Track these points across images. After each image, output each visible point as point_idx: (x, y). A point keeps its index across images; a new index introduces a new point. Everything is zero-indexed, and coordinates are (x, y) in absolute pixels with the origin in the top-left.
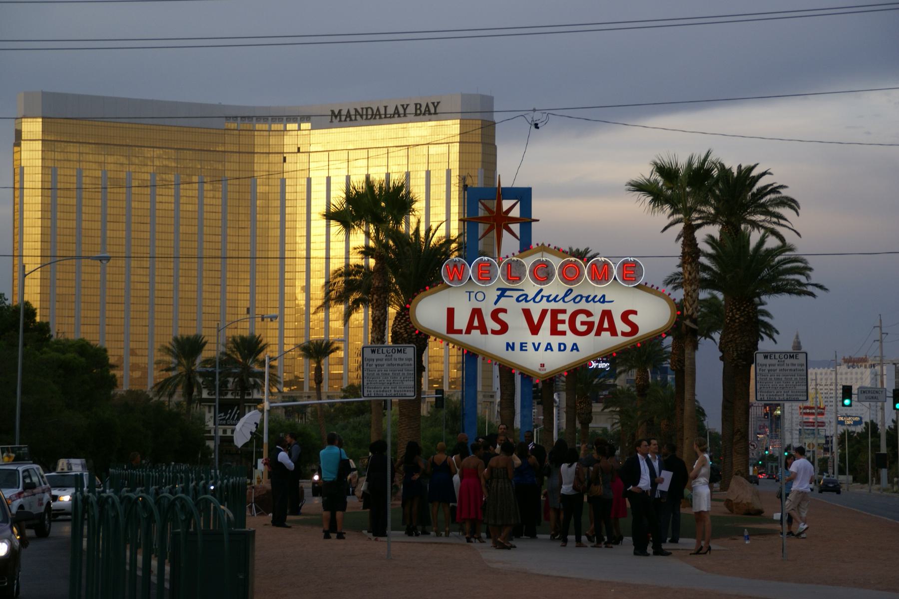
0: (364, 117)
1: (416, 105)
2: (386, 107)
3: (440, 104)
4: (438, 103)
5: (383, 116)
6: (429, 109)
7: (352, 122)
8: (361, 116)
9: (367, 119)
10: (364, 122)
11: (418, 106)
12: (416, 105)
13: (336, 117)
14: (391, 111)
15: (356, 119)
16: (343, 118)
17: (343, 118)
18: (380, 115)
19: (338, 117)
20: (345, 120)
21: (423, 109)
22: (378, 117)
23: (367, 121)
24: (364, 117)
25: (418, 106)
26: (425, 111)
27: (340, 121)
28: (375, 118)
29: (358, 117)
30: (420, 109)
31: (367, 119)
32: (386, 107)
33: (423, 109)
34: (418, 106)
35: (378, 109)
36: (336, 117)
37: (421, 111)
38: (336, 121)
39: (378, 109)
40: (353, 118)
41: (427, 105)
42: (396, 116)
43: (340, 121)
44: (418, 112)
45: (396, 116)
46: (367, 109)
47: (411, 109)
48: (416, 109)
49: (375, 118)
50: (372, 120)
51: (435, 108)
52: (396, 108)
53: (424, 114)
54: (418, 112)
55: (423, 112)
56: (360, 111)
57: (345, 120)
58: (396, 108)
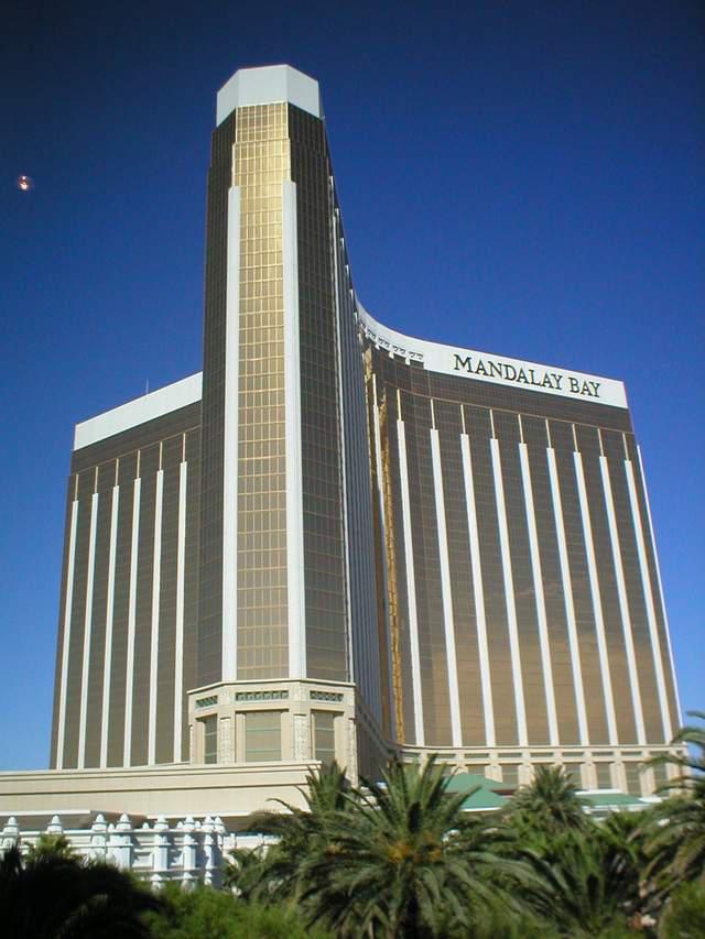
1: (571, 379)
8: (500, 373)
13: (464, 365)
15: (492, 375)
16: (474, 369)
24: (504, 375)
29: (495, 373)
35: (522, 371)
36: (464, 365)
39: (522, 371)
43: (470, 371)
46: (507, 366)
48: (572, 385)
51: (596, 389)
56: (498, 367)
57: (477, 372)
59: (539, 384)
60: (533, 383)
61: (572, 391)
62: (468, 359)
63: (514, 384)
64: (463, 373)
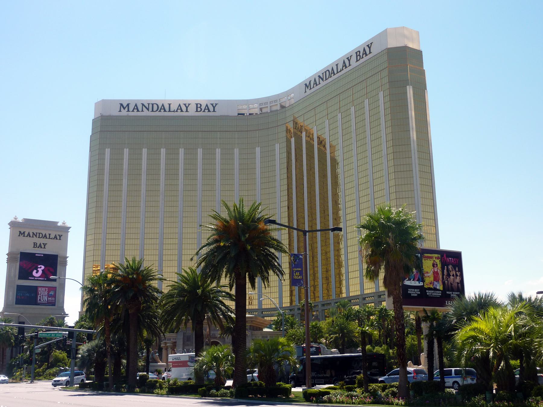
0: (150, 109)
1: (197, 104)
2: (170, 105)
3: (217, 105)
5: (167, 109)
6: (208, 107)
8: (148, 109)
9: (153, 111)
12: (197, 104)
13: (124, 108)
16: (131, 109)
17: (131, 109)
18: (164, 109)
20: (133, 111)
21: (203, 108)
22: (162, 110)
24: (150, 109)
25: (198, 106)
26: (205, 109)
27: (128, 111)
28: (160, 111)
29: (144, 109)
31: (153, 111)
32: (170, 105)
33: (203, 108)
34: (199, 106)
35: (163, 105)
37: (201, 109)
38: (124, 112)
39: (163, 105)
40: (140, 109)
41: (207, 105)
44: (199, 109)
45: (179, 111)
46: (153, 104)
48: (197, 107)
49: (160, 111)
52: (180, 105)
53: (204, 111)
55: (203, 110)
57: (133, 111)
58: (180, 105)
59: (174, 111)
60: (170, 111)
61: (197, 111)
62: (128, 105)
63: (157, 114)
64: (124, 112)
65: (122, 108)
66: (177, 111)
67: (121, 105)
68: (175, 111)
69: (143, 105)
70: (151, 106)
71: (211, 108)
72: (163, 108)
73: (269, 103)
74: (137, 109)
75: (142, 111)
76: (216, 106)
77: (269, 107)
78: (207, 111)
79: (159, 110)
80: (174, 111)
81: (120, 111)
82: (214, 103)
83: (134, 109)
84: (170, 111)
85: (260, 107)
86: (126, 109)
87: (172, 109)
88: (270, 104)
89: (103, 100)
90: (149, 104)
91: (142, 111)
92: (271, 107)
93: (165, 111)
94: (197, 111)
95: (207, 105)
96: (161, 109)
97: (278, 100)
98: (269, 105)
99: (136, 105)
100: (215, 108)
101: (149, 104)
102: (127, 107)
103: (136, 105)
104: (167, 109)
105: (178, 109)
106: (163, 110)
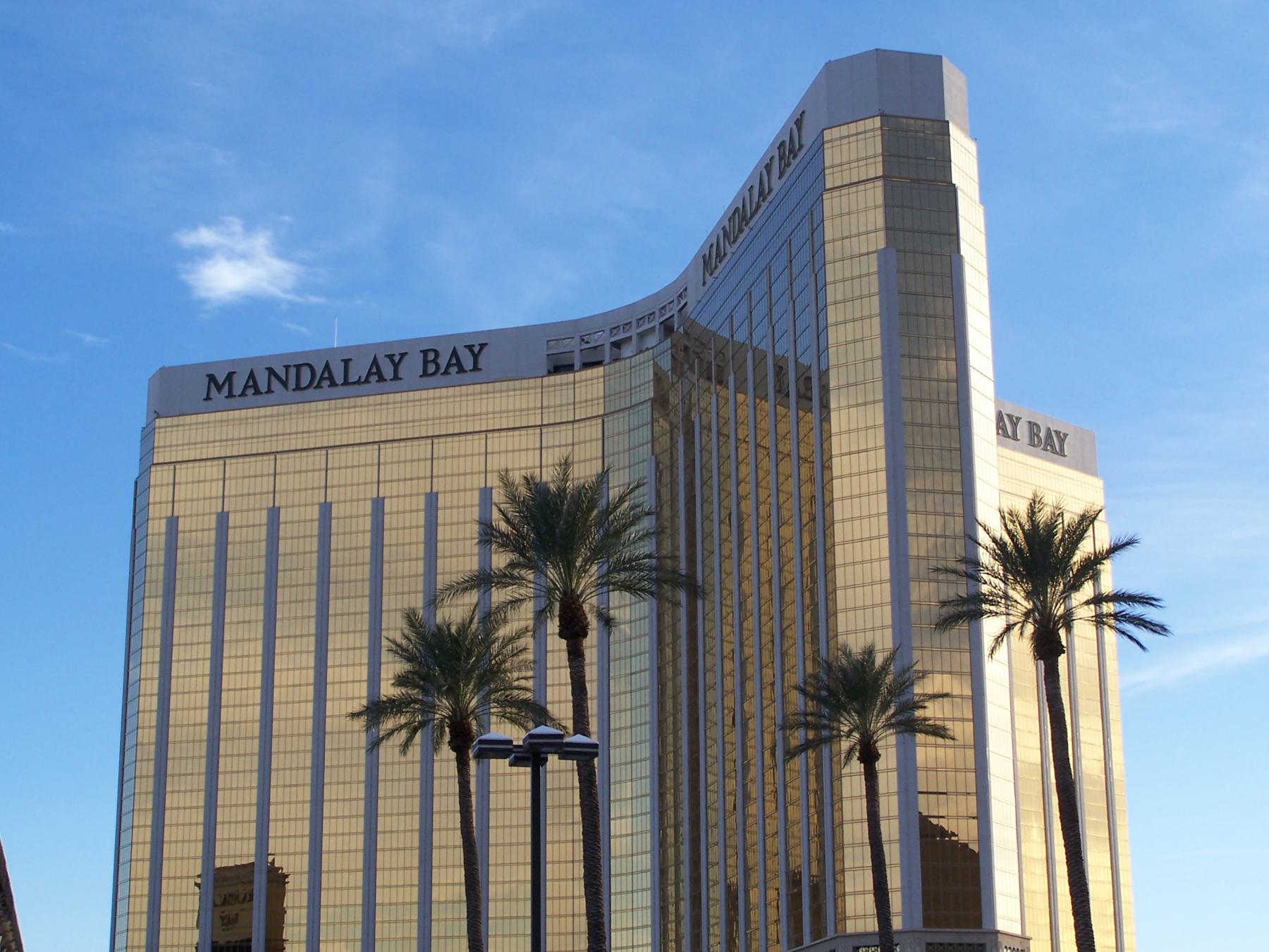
0: (292, 384)
1: (425, 352)
2: (347, 362)
3: (486, 350)
4: (482, 346)
5: (339, 378)
7: (259, 397)
8: (285, 384)
9: (298, 388)
10: (290, 395)
11: (431, 356)
12: (425, 352)
13: (219, 388)
14: (359, 369)
16: (238, 390)
17: (238, 390)
18: (331, 378)
19: (225, 391)
20: (243, 394)
21: (443, 362)
22: (326, 383)
23: (299, 393)
24: (292, 384)
26: (449, 365)
27: (231, 395)
29: (276, 385)
30: (435, 361)
32: (347, 362)
33: (443, 362)
34: (431, 356)
35: (327, 367)
36: (219, 388)
39: (327, 367)
40: (263, 388)
41: (455, 353)
42: (374, 378)
43: (231, 395)
44: (432, 368)
45: (374, 378)
46: (298, 367)
47: (412, 366)
48: (426, 362)
49: (319, 386)
50: (311, 390)
52: (375, 362)
53: (446, 373)
54: (432, 368)
55: (442, 370)
56: (281, 372)
57: (243, 394)
58: (375, 362)
59: (358, 382)
60: (346, 383)
62: (230, 376)
65: (213, 386)
66: (367, 381)
67: (212, 378)
68: (363, 380)
69: (271, 371)
70: (293, 371)
71: (468, 362)
72: (326, 375)
73: (634, 323)
74: (255, 386)
75: (269, 391)
76: (480, 351)
77: (634, 338)
78: (454, 370)
79: (315, 385)
80: (358, 382)
81: (208, 398)
82: (476, 342)
83: (246, 387)
84: (346, 383)
85: (613, 339)
86: (225, 391)
87: (353, 378)
88: (638, 326)
89: (163, 369)
90: (287, 367)
91: (269, 391)
92: (642, 336)
93: (333, 384)
94: (425, 374)
95: (454, 353)
96: (322, 378)
97: (657, 314)
98: (633, 332)
99: (252, 375)
100: (482, 361)
101: (287, 367)
102: (227, 386)
103: (252, 375)
104: (339, 378)
105: (369, 374)
106: (328, 383)
